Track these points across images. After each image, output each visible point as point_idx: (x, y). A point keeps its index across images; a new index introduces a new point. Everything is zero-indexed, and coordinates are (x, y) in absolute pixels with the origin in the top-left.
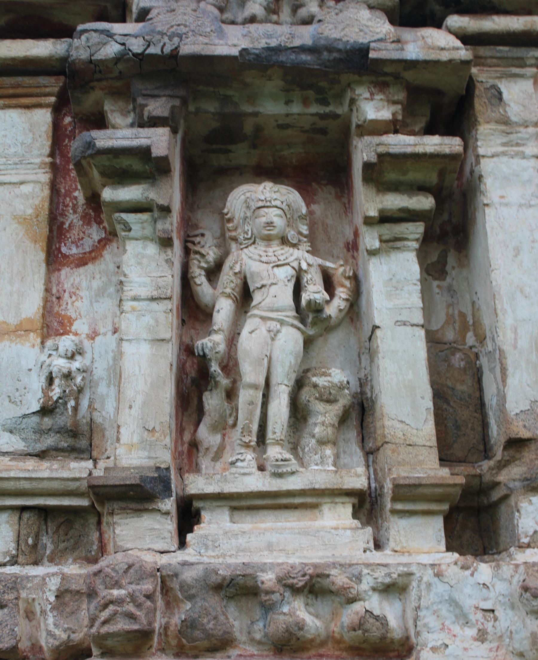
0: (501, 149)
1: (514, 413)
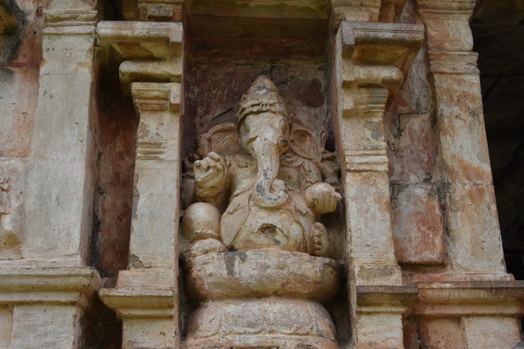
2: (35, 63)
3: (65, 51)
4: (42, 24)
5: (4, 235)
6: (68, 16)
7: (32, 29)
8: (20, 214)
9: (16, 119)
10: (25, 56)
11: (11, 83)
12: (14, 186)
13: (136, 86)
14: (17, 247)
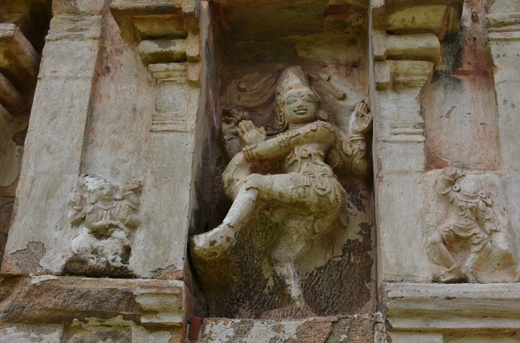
0: (66, 33)
1: (11, 252)
2: (485, 72)
3: (517, 57)
4: (481, 30)
5: (498, 254)
6: (513, 20)
7: (471, 36)
8: (510, 232)
9: (475, 129)
10: (470, 64)
11: (462, 91)
12: (496, 201)
14: (512, 268)
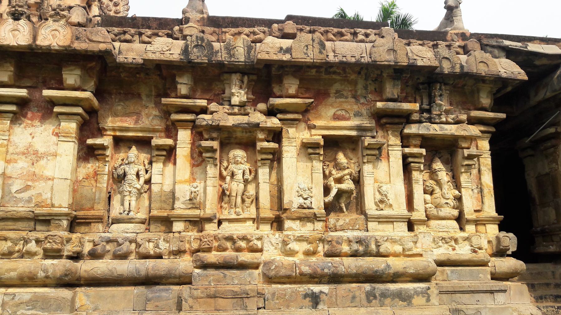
13: (412, 164)
